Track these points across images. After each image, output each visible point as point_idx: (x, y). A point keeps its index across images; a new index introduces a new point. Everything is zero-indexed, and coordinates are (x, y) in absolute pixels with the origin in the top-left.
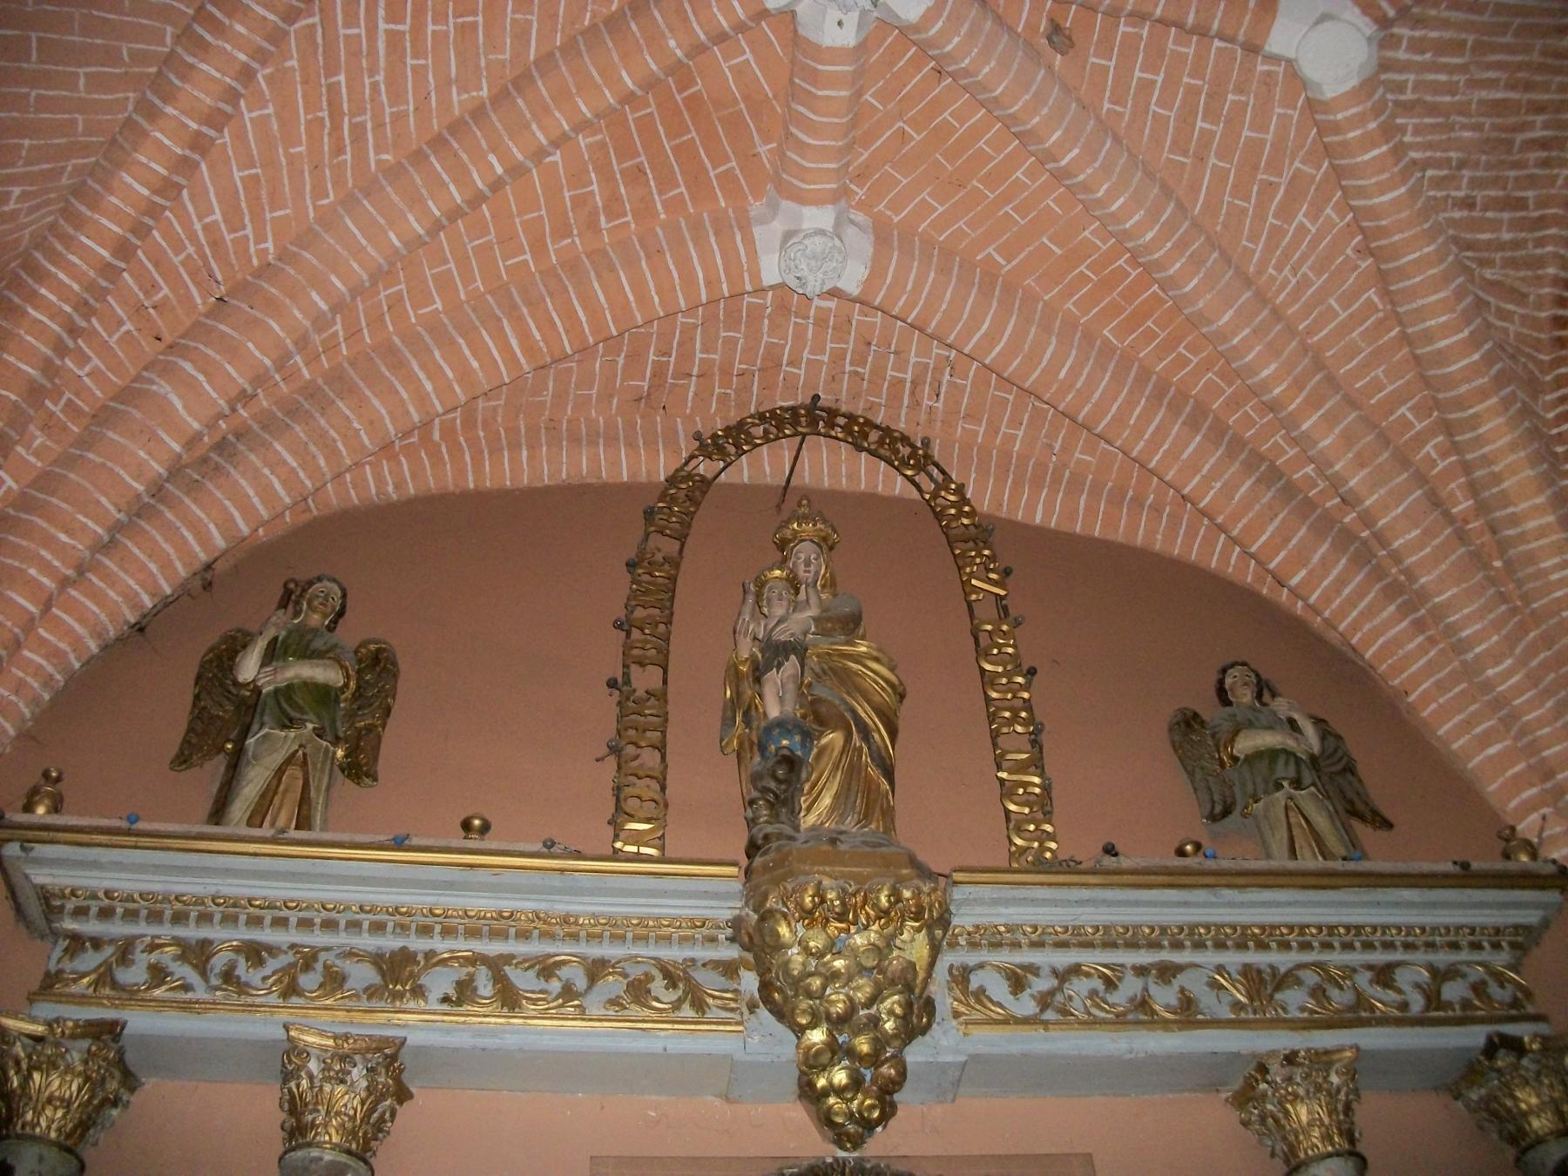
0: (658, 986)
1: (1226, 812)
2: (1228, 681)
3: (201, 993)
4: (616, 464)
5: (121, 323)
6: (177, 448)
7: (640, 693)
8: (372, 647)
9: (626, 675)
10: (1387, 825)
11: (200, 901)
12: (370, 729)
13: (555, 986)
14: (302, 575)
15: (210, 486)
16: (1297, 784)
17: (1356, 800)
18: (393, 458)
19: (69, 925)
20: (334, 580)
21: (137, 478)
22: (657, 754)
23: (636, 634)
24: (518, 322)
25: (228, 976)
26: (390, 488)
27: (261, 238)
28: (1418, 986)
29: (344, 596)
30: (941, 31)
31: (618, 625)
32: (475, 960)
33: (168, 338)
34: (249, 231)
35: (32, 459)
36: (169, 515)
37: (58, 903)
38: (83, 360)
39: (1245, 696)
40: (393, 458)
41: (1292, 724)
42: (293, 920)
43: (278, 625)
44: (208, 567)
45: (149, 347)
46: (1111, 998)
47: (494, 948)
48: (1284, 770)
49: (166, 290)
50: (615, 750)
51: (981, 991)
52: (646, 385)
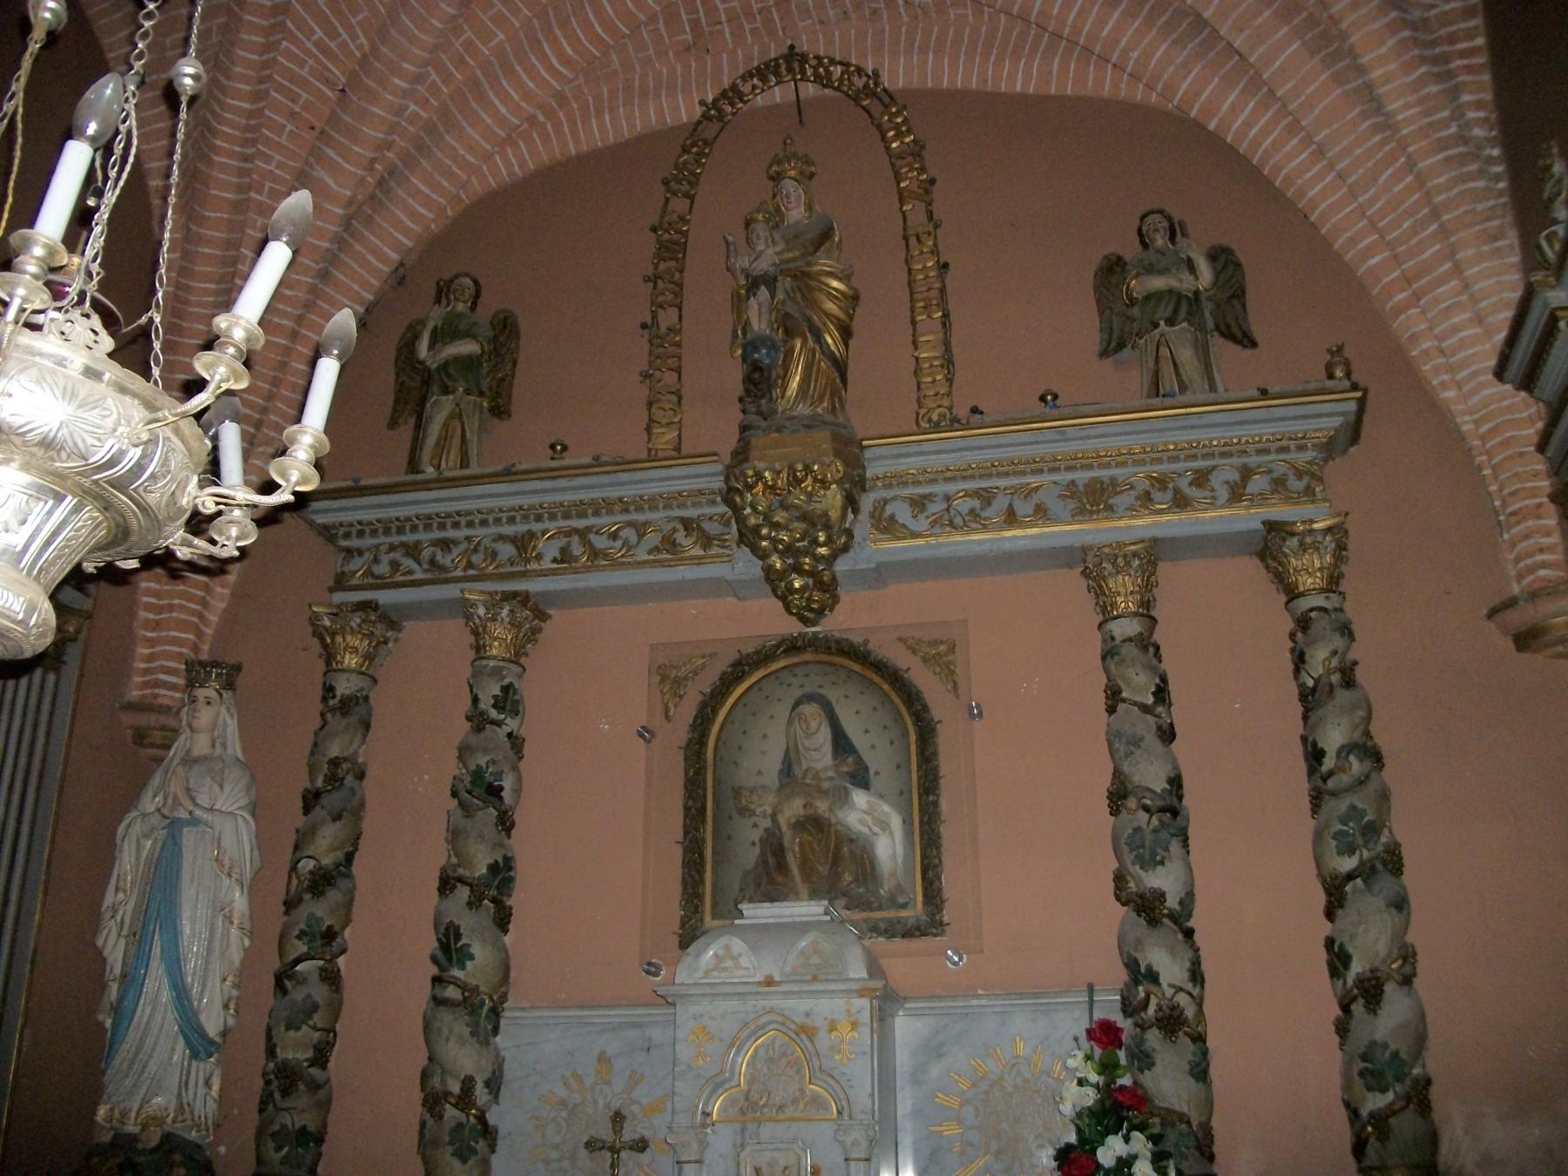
0: (680, 536)
1: (1121, 345)
2: (1144, 229)
3: (419, 575)
4: (676, 109)
5: (284, 126)
6: (340, 211)
7: (663, 330)
8: (501, 317)
9: (654, 316)
10: (1254, 344)
11: (408, 519)
12: (503, 380)
13: (619, 543)
14: (447, 275)
15: (378, 219)
16: (1171, 322)
17: (1233, 324)
18: (514, 144)
19: (344, 543)
20: (467, 275)
21: (321, 238)
22: (675, 376)
23: (660, 284)
24: (554, 42)
25: (433, 562)
26: (516, 168)
27: (354, 37)
28: (1227, 482)
29: (476, 283)
31: (647, 280)
32: (568, 533)
33: (318, 125)
34: (345, 36)
36: (358, 247)
38: (267, 159)
39: (1160, 241)
40: (514, 144)
41: (1191, 266)
42: (463, 523)
43: (436, 315)
44: (402, 264)
45: (308, 136)
46: (984, 514)
47: (581, 523)
48: (1164, 311)
49: (304, 95)
50: (646, 376)
51: (892, 518)
52: (689, 37)
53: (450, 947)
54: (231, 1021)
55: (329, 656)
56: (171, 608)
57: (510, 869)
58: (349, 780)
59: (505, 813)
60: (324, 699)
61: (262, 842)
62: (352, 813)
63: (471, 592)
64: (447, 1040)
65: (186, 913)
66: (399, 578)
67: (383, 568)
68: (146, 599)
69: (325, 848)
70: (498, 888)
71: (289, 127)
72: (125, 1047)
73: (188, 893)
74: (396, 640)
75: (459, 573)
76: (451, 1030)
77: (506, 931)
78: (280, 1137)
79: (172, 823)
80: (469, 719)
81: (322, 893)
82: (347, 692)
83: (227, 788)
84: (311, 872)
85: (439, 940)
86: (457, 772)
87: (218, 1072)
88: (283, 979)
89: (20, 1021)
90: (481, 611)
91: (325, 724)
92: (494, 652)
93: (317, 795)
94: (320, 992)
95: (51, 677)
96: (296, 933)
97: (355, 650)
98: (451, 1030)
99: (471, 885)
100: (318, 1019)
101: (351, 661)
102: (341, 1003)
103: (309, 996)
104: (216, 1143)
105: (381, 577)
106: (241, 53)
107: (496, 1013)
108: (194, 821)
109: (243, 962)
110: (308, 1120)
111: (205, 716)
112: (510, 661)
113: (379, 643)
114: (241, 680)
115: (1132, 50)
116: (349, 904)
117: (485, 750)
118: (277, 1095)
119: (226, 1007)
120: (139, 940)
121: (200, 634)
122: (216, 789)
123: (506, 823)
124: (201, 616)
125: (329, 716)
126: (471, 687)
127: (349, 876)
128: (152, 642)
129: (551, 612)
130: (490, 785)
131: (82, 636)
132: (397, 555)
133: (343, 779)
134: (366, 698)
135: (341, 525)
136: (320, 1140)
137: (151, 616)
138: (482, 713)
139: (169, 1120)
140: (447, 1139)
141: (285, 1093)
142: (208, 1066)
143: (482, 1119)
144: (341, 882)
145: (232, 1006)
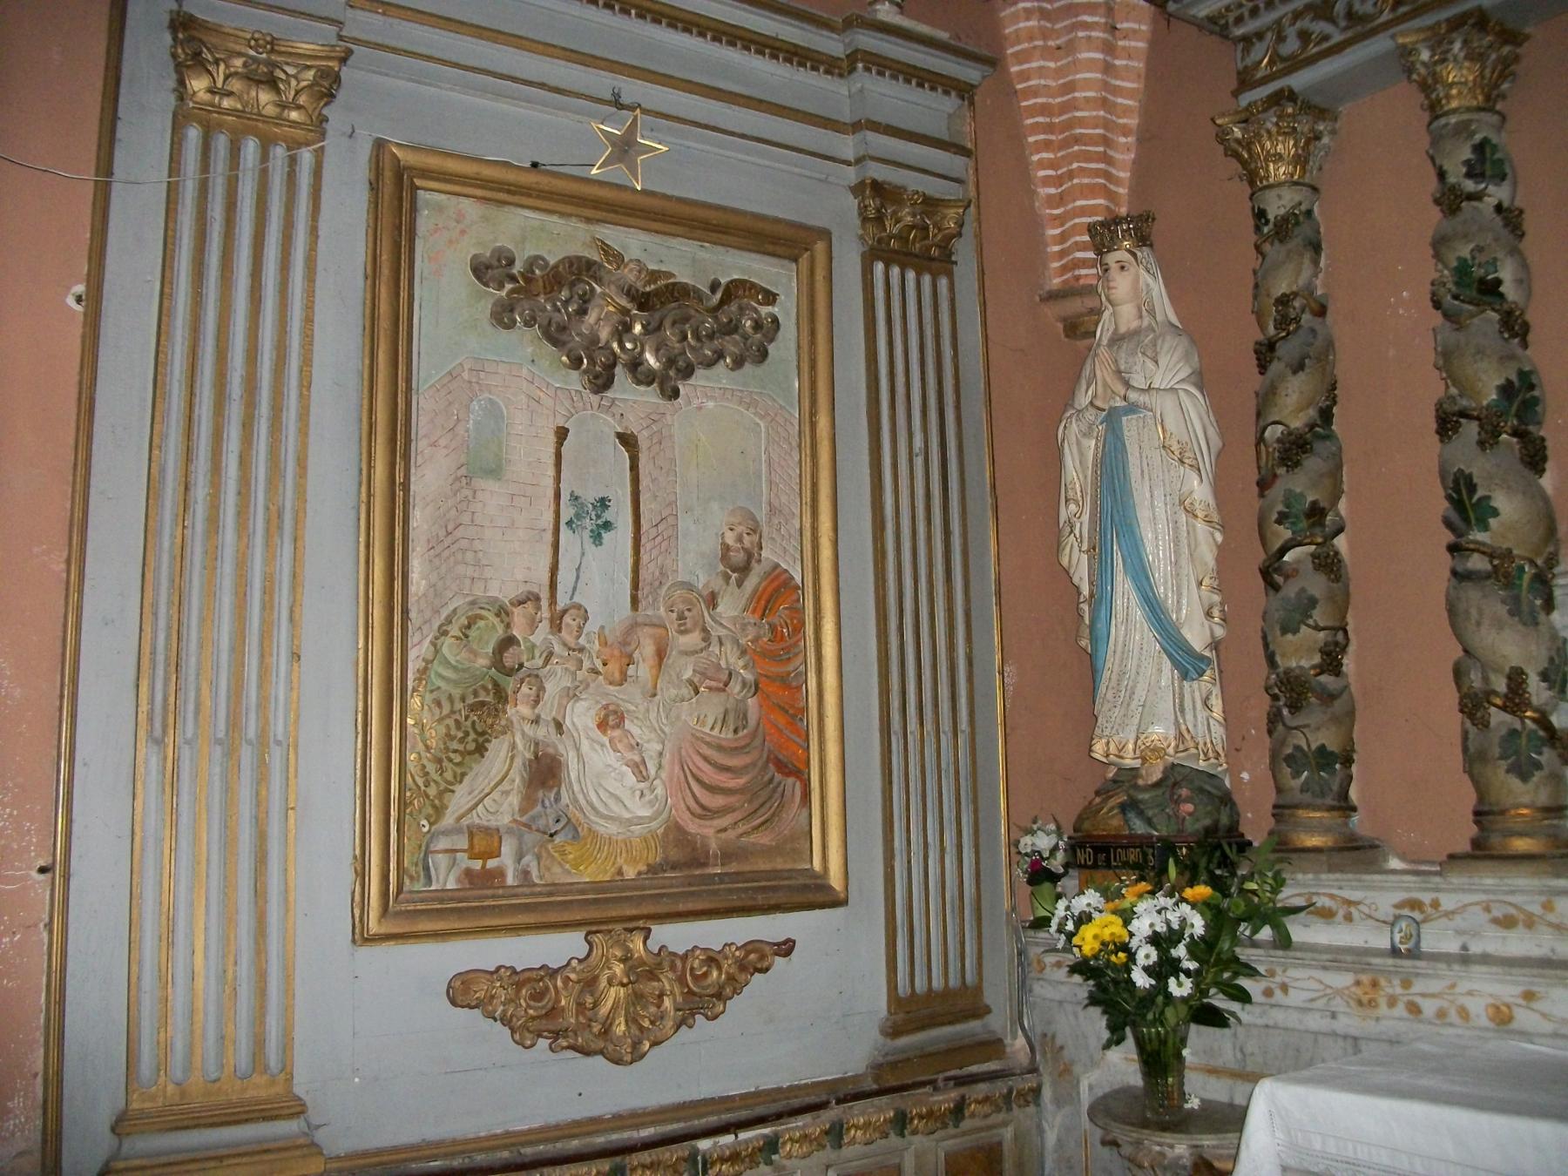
3: (1338, 38)
19: (1239, 32)
37: (1223, 22)
53: (1466, 505)
54: (1220, 632)
55: (1252, 177)
56: (1071, 175)
57: (1532, 387)
58: (1306, 318)
59: (1509, 313)
60: (1258, 229)
61: (1221, 412)
62: (1318, 358)
63: (1403, 34)
64: (1478, 624)
65: (1143, 514)
66: (1313, 50)
67: (1291, 46)
68: (1042, 173)
69: (1293, 406)
70: (1517, 415)
72: (1106, 674)
73: (1140, 491)
74: (1333, 132)
75: (1386, 16)
76: (1480, 612)
77: (1541, 471)
78: (1296, 760)
79: (1109, 414)
80: (1437, 202)
81: (1297, 464)
82: (1282, 211)
83: (1163, 361)
84: (1279, 441)
85: (1449, 498)
86: (1437, 275)
87: (1216, 691)
88: (1271, 573)
89: (998, 657)
90: (1425, 55)
91: (1263, 256)
92: (1454, 104)
93: (1271, 346)
94: (1317, 585)
95: (943, 283)
96: (1275, 516)
97: (1279, 158)
98: (1480, 612)
99: (1478, 418)
100: (1319, 616)
101: (1279, 172)
102: (1347, 594)
103: (1303, 590)
104: (1234, 771)
105: (1292, 57)
107: (1543, 583)
108: (1133, 408)
109: (1218, 560)
110: (1327, 738)
111: (1121, 284)
112: (1479, 109)
113: (1307, 143)
114: (1157, 230)
116: (1336, 473)
117: (1466, 237)
118: (1285, 712)
119: (1209, 615)
120: (1099, 553)
121: (1111, 196)
122: (1150, 364)
123: (1515, 326)
124: (1108, 176)
125: (1267, 247)
126: (1432, 159)
127: (1330, 436)
128: (1060, 220)
129: (1528, 30)
130: (1482, 281)
131: (968, 230)
132: (1305, 23)
133: (1297, 320)
134: (1309, 213)
135: (1228, 9)
136: (1348, 761)
137: (1052, 191)
138: (1453, 188)
139: (1171, 751)
140: (1497, 751)
141: (1295, 707)
142: (1206, 683)
143: (1543, 721)
144: (1319, 446)
145: (1216, 612)
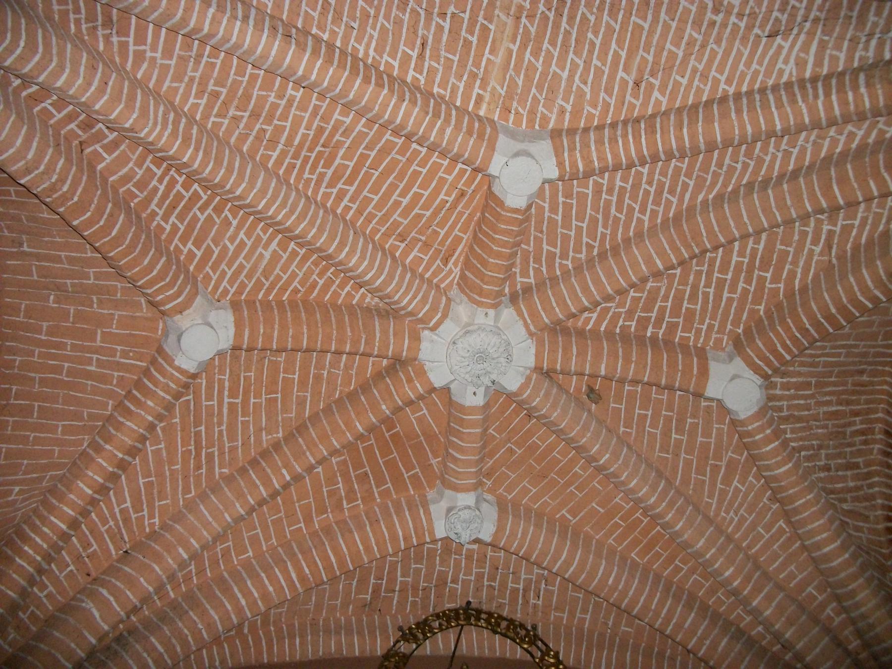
4: (351, 645)
6: (93, 641)
27: (151, 516)
30: (682, 527)
33: (94, 574)
34: (145, 513)
35: (7, 647)
45: (81, 579)
49: (95, 546)
52: (369, 597)
71: (72, 567)
106: (81, 485)
115: (706, 639)
